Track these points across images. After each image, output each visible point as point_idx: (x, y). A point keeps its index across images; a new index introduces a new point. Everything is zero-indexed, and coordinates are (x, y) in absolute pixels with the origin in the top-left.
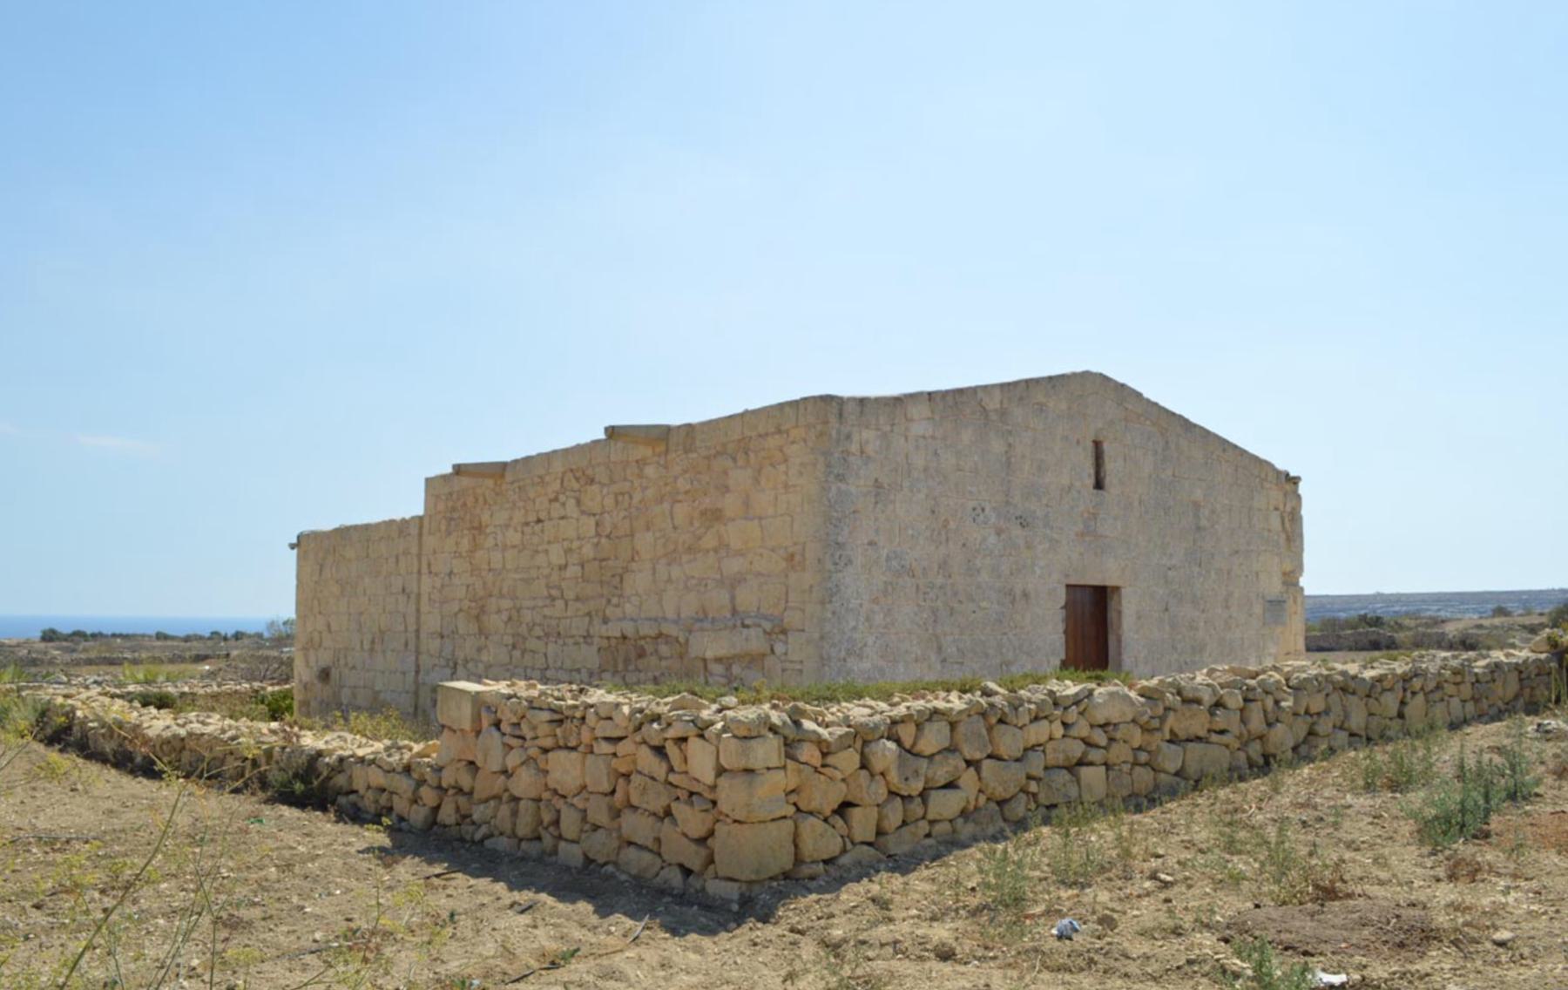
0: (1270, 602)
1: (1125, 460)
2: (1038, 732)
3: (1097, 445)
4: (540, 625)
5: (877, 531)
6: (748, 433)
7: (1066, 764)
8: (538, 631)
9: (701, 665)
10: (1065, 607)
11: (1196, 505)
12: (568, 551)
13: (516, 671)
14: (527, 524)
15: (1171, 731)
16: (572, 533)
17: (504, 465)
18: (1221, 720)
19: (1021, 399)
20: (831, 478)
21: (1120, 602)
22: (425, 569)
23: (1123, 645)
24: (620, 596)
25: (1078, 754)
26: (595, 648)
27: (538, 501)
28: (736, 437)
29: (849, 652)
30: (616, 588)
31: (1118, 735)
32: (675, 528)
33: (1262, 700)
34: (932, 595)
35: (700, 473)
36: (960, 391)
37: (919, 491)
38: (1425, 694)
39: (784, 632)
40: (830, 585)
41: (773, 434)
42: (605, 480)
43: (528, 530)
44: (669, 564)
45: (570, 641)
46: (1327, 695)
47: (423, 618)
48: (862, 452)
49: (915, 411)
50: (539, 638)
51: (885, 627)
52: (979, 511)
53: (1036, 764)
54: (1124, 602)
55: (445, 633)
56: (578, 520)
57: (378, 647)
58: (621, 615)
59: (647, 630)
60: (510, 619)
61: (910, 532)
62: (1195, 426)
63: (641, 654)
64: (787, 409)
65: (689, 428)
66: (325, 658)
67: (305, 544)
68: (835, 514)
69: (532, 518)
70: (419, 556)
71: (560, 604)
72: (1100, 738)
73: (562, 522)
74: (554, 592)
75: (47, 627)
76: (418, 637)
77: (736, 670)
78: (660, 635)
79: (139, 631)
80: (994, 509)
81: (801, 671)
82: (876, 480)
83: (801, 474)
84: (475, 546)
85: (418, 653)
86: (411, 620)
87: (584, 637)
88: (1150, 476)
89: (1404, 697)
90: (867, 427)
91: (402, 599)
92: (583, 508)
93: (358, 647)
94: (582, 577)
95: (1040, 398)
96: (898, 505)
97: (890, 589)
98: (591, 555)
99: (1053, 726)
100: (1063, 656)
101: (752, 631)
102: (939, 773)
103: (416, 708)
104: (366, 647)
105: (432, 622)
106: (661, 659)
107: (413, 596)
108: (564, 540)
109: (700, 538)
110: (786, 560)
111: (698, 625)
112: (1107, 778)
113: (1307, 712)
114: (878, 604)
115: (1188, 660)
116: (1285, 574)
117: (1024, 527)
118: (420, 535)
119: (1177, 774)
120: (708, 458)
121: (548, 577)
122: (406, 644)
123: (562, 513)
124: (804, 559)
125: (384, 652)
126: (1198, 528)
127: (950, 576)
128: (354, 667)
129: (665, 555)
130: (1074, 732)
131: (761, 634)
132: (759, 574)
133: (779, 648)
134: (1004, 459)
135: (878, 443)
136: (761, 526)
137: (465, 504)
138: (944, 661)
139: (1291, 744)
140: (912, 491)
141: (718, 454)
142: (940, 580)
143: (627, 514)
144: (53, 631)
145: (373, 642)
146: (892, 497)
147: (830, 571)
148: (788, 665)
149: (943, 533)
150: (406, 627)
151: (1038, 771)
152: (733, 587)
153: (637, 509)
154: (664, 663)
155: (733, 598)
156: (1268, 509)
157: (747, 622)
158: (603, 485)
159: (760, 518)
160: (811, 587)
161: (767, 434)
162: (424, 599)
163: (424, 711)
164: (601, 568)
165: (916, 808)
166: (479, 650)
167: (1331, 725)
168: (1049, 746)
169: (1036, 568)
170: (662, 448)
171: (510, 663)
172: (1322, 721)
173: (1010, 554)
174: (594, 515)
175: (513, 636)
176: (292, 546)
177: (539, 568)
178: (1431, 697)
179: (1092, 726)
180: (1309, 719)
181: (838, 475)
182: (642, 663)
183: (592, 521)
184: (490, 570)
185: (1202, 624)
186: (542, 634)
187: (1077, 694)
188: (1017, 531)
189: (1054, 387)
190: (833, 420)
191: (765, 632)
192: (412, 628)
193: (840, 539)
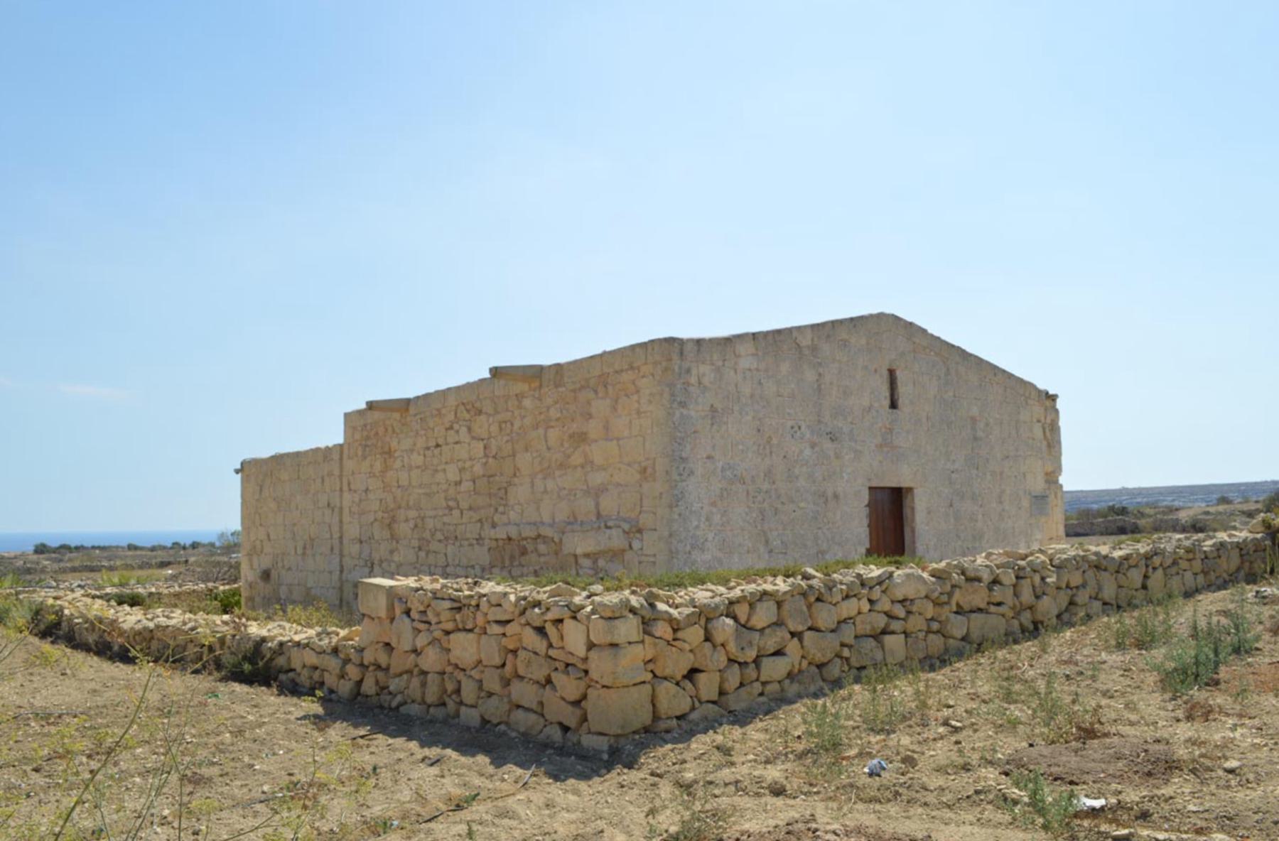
0: (1036, 497)
1: (914, 384)
2: (849, 608)
3: (892, 373)
4: (440, 530)
5: (714, 447)
6: (606, 370)
7: (872, 633)
8: (439, 536)
9: (572, 560)
10: (868, 505)
11: (973, 420)
12: (462, 470)
13: (422, 568)
14: (428, 448)
15: (958, 605)
16: (465, 455)
17: (408, 401)
18: (998, 594)
19: (828, 336)
20: (675, 405)
21: (913, 500)
22: (345, 488)
23: (917, 534)
24: (505, 505)
25: (882, 625)
26: (486, 548)
27: (436, 429)
28: (597, 373)
29: (693, 547)
30: (502, 499)
31: (914, 609)
32: (549, 449)
33: (1031, 578)
34: (760, 498)
35: (568, 403)
36: (779, 332)
37: (747, 414)
38: (1164, 569)
39: (640, 531)
40: (676, 492)
41: (627, 370)
42: (491, 411)
43: (428, 453)
44: (545, 478)
45: (466, 543)
46: (1084, 572)
47: (345, 527)
49: (742, 349)
50: (440, 541)
52: (796, 428)
53: (848, 634)
54: (916, 500)
55: (363, 539)
56: (469, 444)
57: (309, 552)
58: (506, 521)
59: (529, 532)
60: (416, 526)
61: (741, 447)
62: (971, 355)
63: (524, 552)
64: (638, 349)
65: (558, 367)
66: (266, 562)
67: (248, 469)
69: (432, 443)
70: (341, 476)
71: (456, 513)
72: (900, 611)
73: (457, 447)
74: (451, 504)
75: (38, 542)
76: (341, 543)
77: (601, 563)
78: (539, 536)
79: (114, 544)
80: (808, 427)
81: (654, 563)
82: (712, 406)
83: (650, 402)
84: (386, 468)
85: (342, 555)
86: (336, 529)
87: (477, 540)
88: (935, 397)
89: (1147, 571)
90: (703, 363)
91: (328, 512)
92: (474, 434)
93: (293, 552)
94: (474, 490)
95: (844, 336)
96: (730, 426)
97: (725, 493)
98: (481, 473)
99: (861, 602)
100: (868, 546)
101: (614, 532)
102: (769, 643)
103: (341, 600)
104: (300, 551)
105: (352, 531)
106: (540, 555)
107: (336, 510)
108: (458, 461)
109: (569, 457)
110: (640, 473)
111: (569, 527)
112: (906, 644)
113: (1068, 586)
114: (716, 506)
115: (970, 546)
116: (1047, 474)
118: (341, 459)
119: (963, 639)
120: (574, 391)
121: (446, 491)
122: (332, 549)
123: (457, 439)
124: (655, 472)
125: (314, 555)
126: (975, 439)
127: (774, 483)
128: (289, 569)
129: (542, 471)
130: (878, 607)
131: (621, 534)
132: (618, 485)
133: (636, 545)
135: (712, 375)
136: (619, 445)
137: (377, 434)
138: (771, 551)
139: (1055, 612)
140: (741, 414)
141: (582, 388)
142: (766, 486)
143: (509, 438)
144: (44, 546)
145: (305, 548)
146: (725, 419)
147: (675, 481)
148: (643, 558)
149: (768, 447)
150: (331, 535)
151: (849, 639)
152: (597, 496)
153: (518, 434)
154: (542, 559)
155: (597, 505)
156: (1032, 422)
157: (610, 524)
158: (489, 415)
159: (618, 439)
160: (661, 494)
161: (622, 371)
162: (346, 511)
163: (348, 603)
164: (489, 482)
165: (751, 672)
166: (392, 552)
167: (1087, 596)
168: (858, 619)
170: (537, 384)
171: (417, 562)
172: (1080, 593)
173: (823, 464)
174: (483, 440)
175: (419, 539)
176: (237, 471)
177: (438, 484)
178: (1169, 571)
179: (893, 602)
180: (1069, 592)
181: (681, 402)
182: (524, 560)
183: (481, 445)
184: (399, 487)
185: (980, 517)
186: (442, 538)
187: (880, 576)
188: (828, 445)
189: (855, 326)
190: (675, 357)
191: (624, 532)
192: (336, 536)
193: (684, 455)
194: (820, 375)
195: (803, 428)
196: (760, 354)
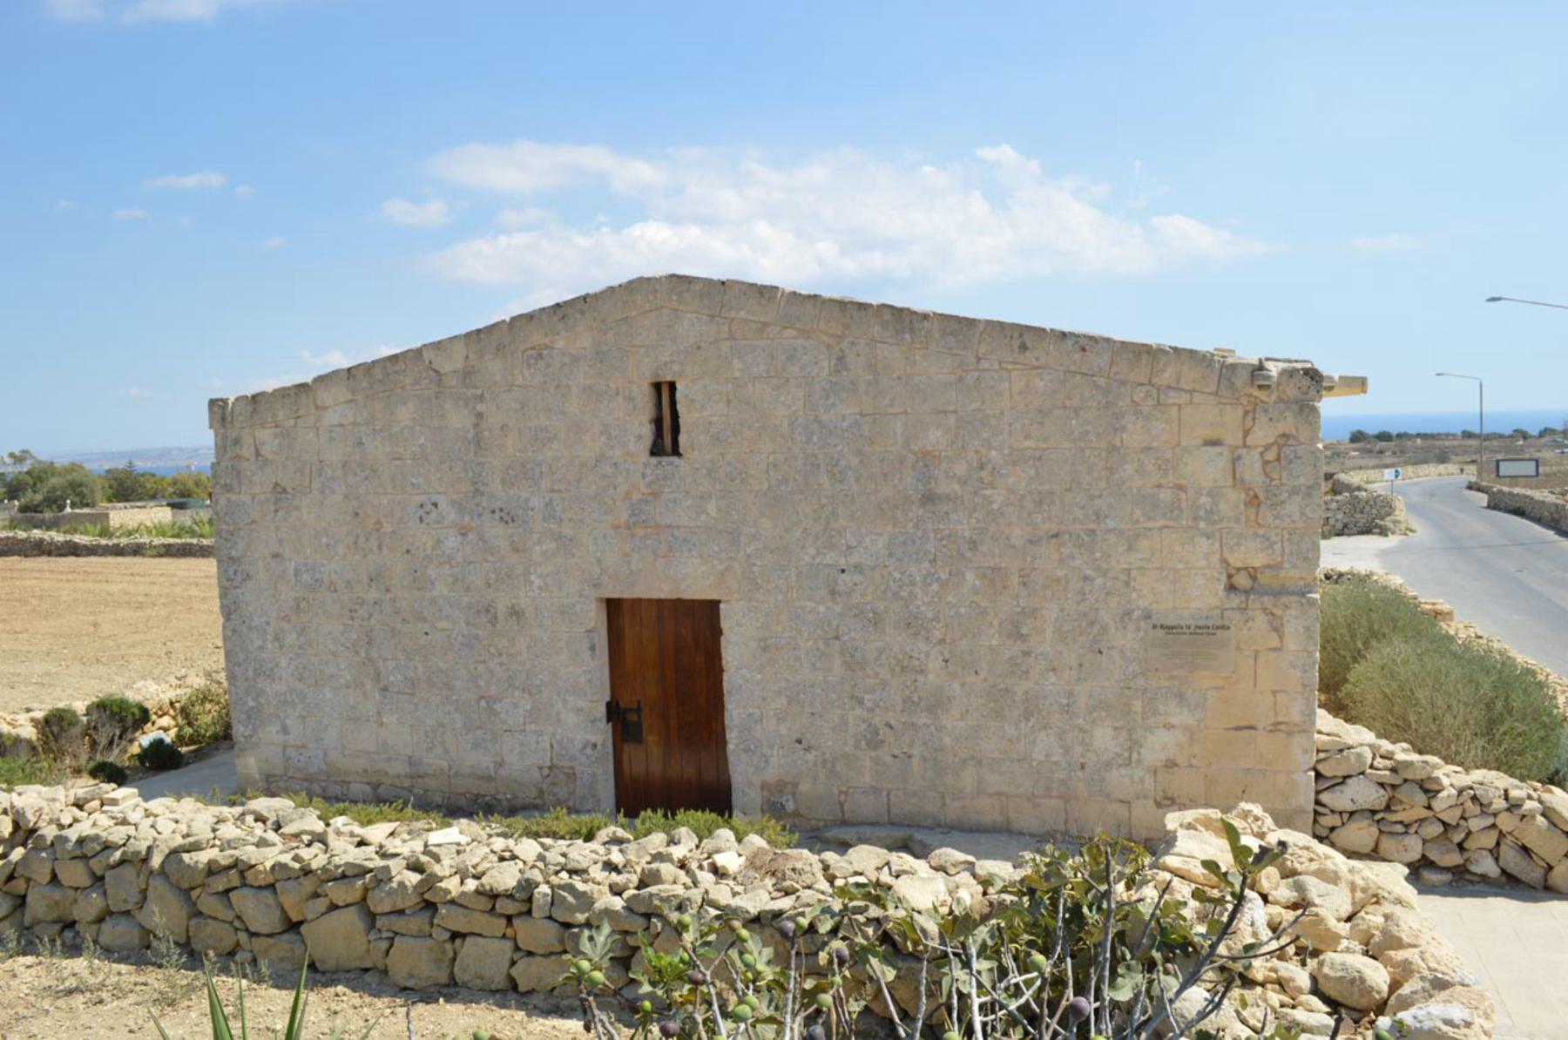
3: (664, 392)
5: (281, 542)
11: (927, 460)
37: (333, 492)
48: (258, 454)
51: (300, 648)
52: (429, 507)
68: (225, 527)
75: (1355, 429)
79: (1442, 431)
80: (453, 503)
95: (537, 338)
97: (303, 605)
114: (289, 621)
117: (507, 523)
126: (928, 498)
134: (470, 436)
142: (373, 595)
144: (1360, 433)
169: (533, 578)
181: (226, 485)
188: (497, 533)
194: (480, 415)
195: (443, 504)
196: (359, 398)
